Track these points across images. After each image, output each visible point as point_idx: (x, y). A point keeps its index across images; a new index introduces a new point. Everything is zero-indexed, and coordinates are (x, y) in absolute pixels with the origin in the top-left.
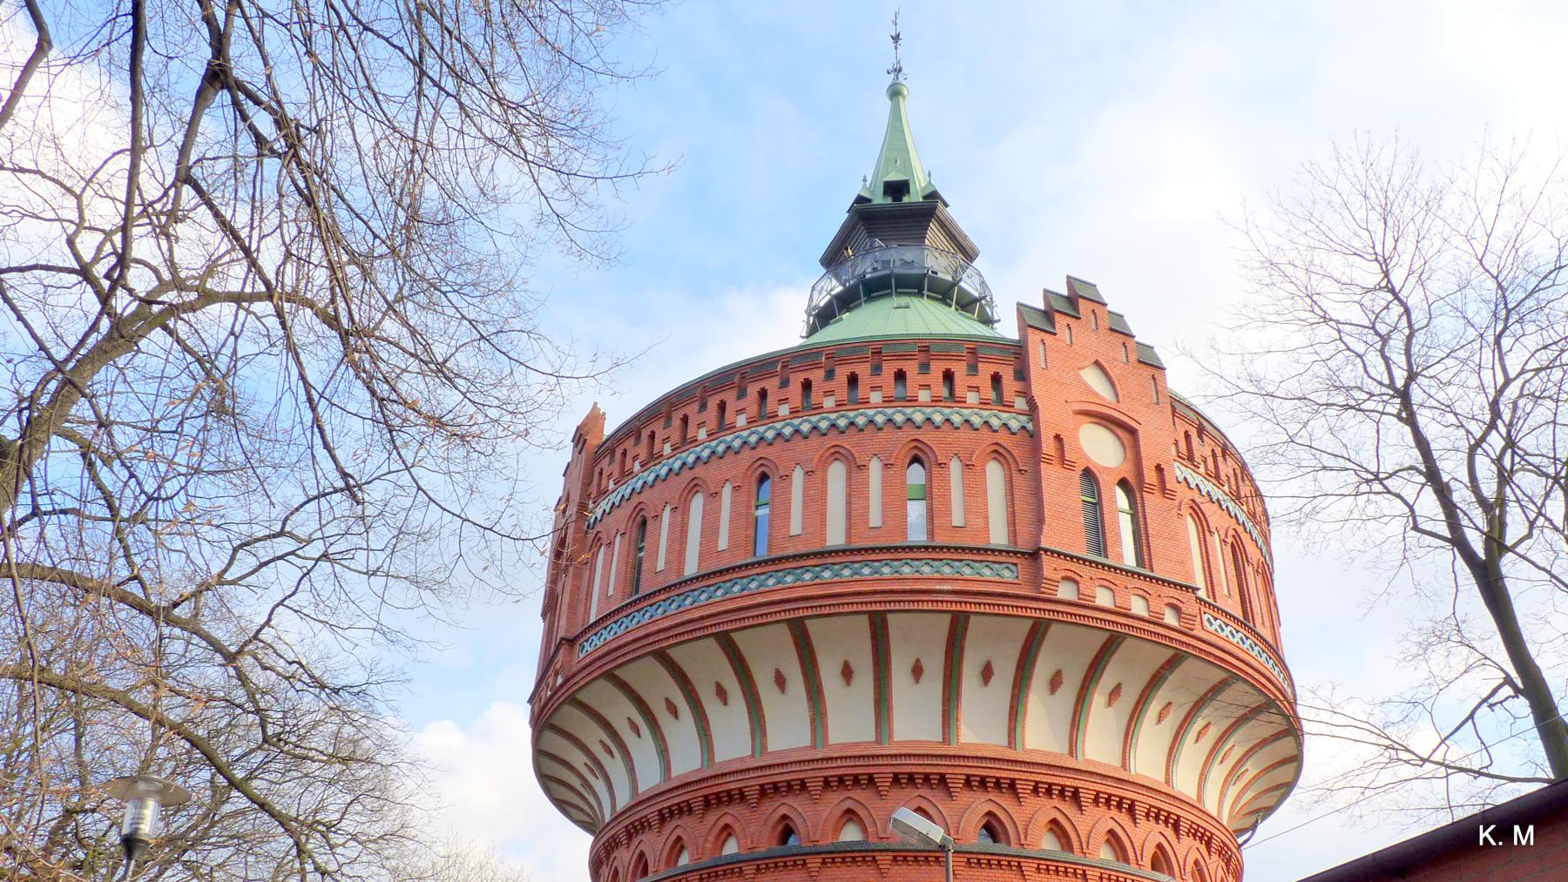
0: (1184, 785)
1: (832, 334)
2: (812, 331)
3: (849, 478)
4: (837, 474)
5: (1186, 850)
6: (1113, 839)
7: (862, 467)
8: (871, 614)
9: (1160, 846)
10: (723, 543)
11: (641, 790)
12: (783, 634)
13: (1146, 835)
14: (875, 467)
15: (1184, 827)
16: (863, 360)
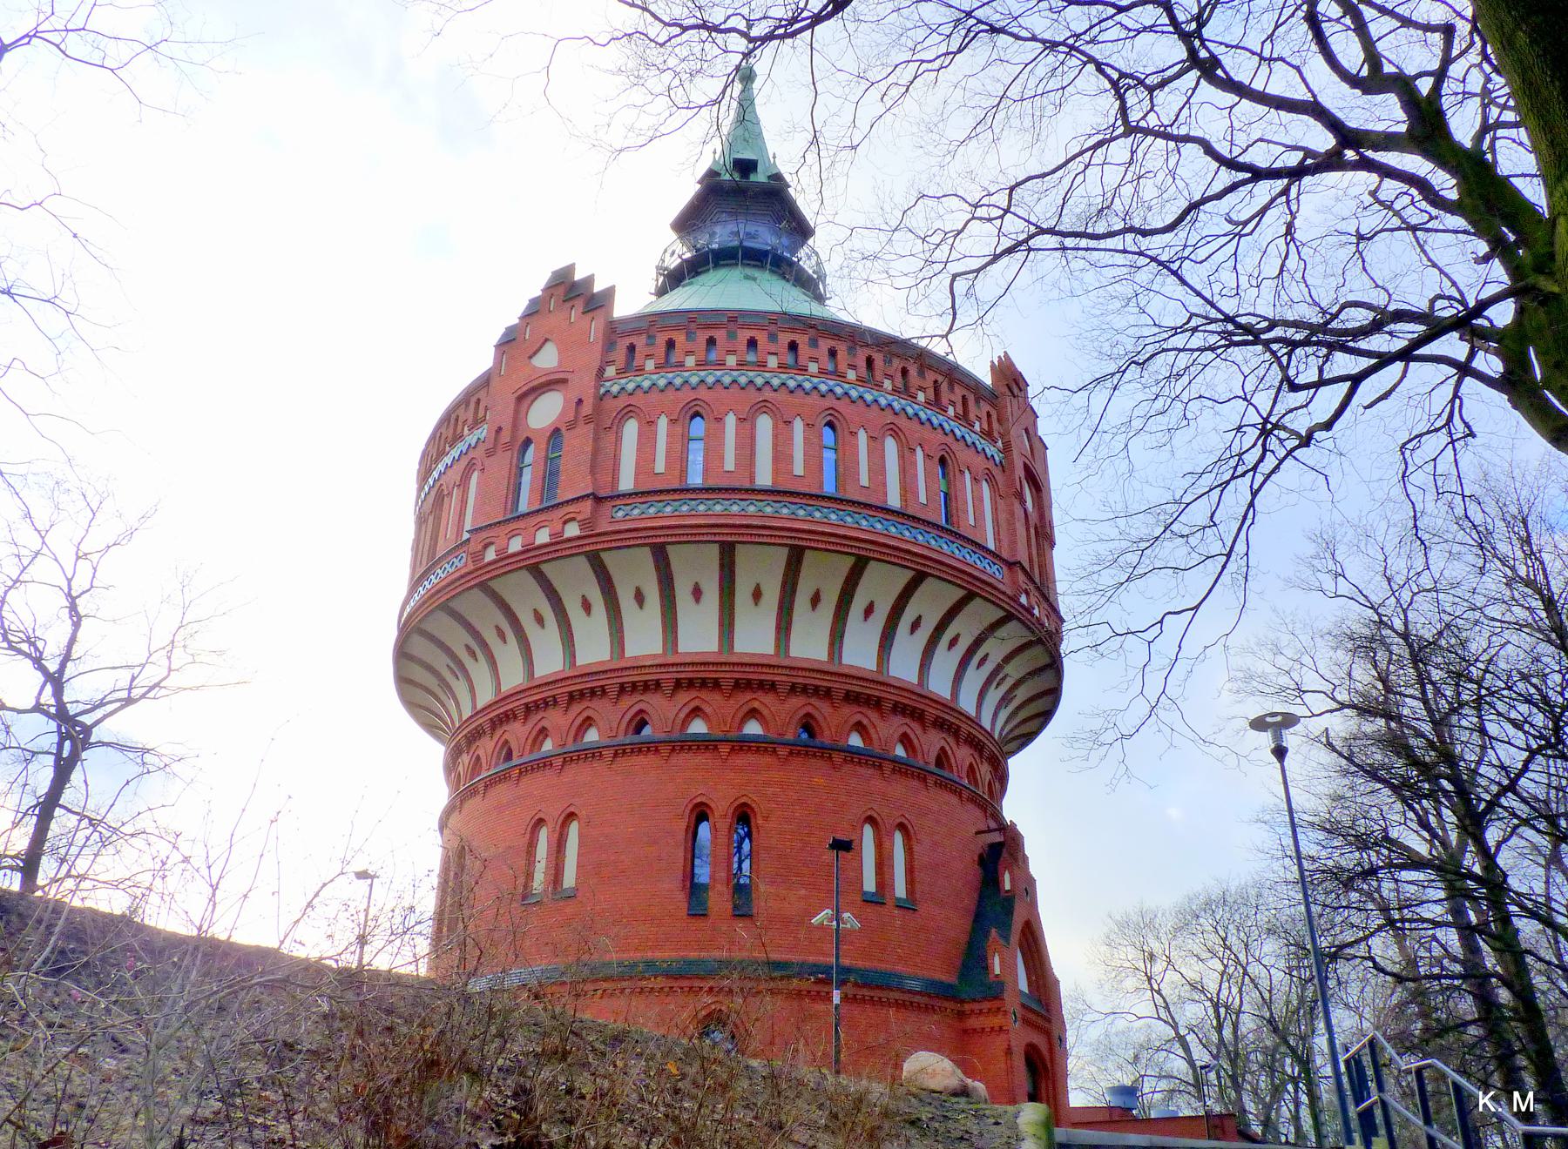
0: (967, 703)
1: (684, 299)
2: (661, 292)
3: (775, 427)
4: (764, 424)
5: (963, 755)
6: (905, 740)
7: (788, 423)
8: (722, 543)
9: (942, 748)
10: (660, 466)
11: (503, 689)
12: (645, 555)
13: (932, 742)
14: (798, 425)
15: (963, 734)
16: (804, 332)
